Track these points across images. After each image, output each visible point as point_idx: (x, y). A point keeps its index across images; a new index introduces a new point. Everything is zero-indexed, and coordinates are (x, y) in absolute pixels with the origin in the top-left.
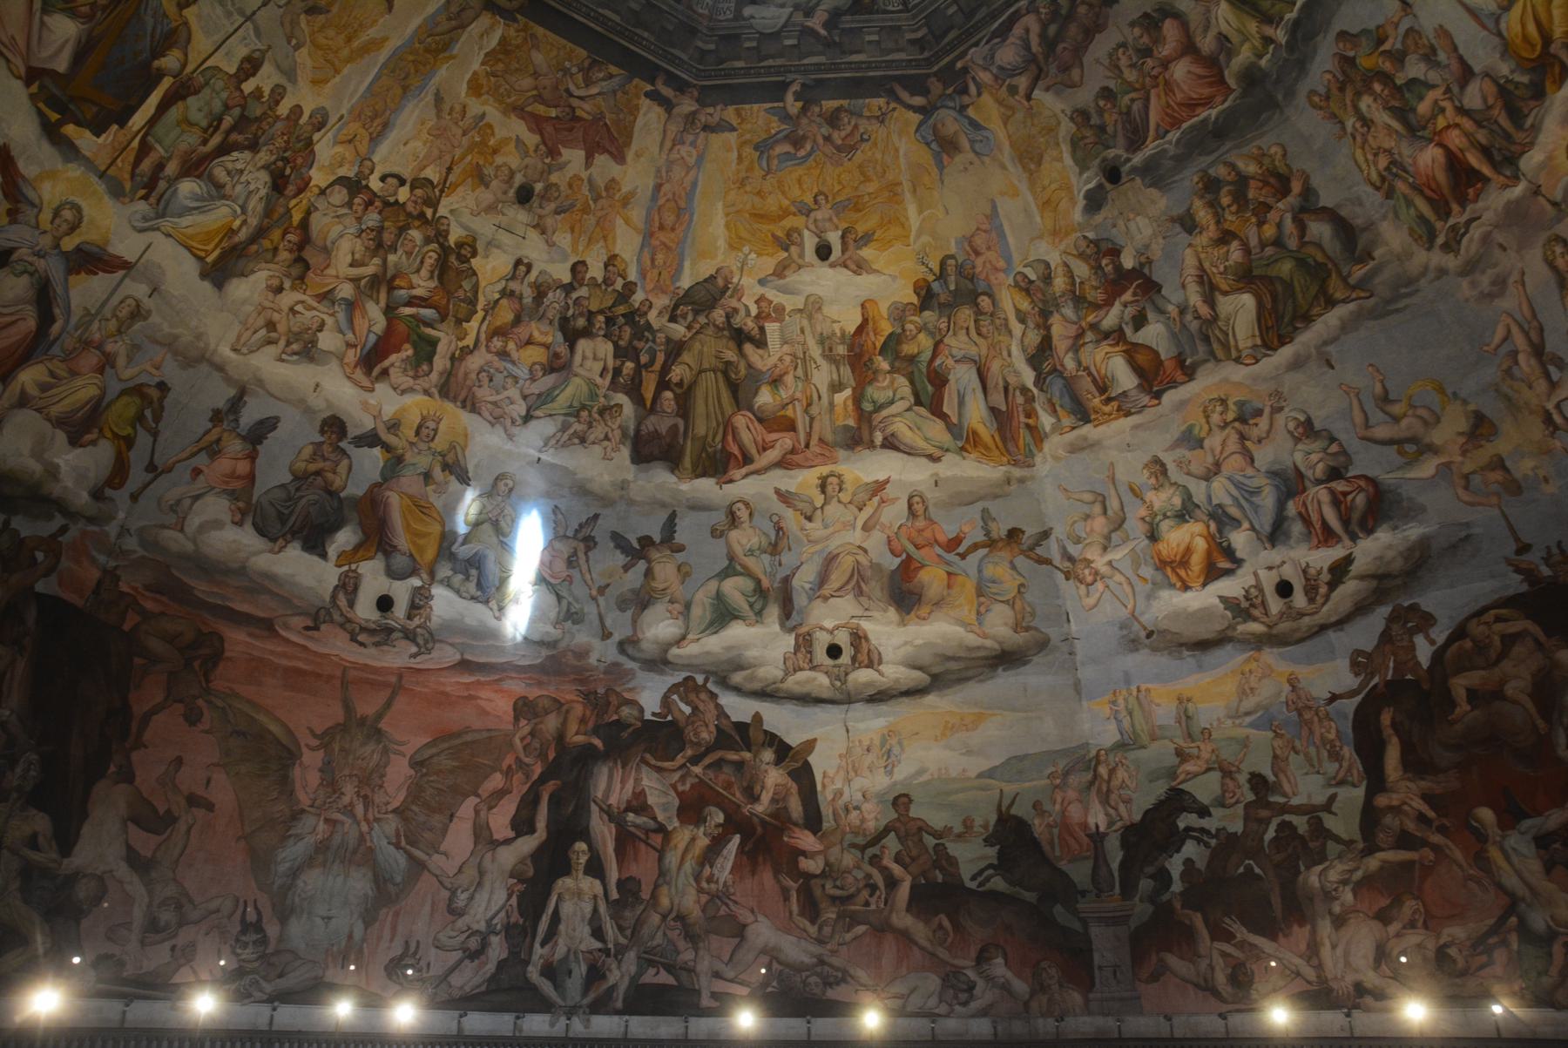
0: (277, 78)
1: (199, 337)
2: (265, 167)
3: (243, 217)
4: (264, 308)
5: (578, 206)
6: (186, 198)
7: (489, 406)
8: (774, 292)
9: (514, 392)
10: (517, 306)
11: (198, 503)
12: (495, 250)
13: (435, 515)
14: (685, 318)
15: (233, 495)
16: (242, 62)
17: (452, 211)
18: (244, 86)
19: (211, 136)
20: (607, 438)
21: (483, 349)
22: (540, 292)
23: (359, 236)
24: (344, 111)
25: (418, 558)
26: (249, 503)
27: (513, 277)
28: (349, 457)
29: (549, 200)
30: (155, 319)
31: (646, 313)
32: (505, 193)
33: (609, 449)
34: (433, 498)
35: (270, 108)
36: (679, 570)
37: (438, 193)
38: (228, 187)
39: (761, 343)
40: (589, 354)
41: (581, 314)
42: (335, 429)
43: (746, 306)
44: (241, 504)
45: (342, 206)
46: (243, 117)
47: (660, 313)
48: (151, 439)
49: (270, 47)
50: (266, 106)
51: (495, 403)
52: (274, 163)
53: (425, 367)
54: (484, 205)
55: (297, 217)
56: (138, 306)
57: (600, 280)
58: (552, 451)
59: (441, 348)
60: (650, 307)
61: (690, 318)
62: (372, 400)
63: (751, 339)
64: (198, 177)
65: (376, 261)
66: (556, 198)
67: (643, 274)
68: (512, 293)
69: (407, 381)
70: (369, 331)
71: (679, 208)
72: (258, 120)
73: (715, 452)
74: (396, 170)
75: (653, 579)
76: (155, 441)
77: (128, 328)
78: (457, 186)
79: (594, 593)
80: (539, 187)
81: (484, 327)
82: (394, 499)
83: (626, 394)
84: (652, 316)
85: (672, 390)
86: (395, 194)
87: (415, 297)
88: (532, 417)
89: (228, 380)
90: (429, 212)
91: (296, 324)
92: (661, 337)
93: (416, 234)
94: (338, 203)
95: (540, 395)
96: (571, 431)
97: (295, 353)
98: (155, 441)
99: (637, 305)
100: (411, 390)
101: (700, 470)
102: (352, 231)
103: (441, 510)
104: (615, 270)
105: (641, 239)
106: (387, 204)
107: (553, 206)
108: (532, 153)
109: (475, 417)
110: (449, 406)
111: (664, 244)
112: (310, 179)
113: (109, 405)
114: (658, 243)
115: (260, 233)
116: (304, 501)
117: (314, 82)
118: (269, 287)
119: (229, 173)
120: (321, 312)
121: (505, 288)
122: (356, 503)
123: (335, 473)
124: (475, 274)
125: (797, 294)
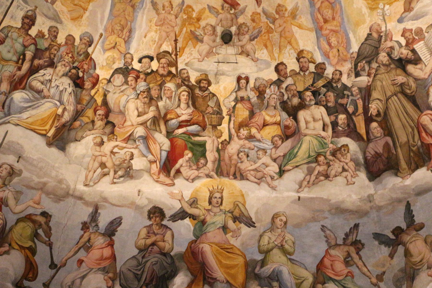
0: (49, 23)
1: (60, 181)
2: (64, 75)
3: (63, 107)
4: (96, 156)
5: (264, 31)
6: (21, 102)
7: (252, 172)
8: (411, 22)
9: (266, 159)
10: (249, 106)
11: (85, 280)
12: (222, 77)
13: (238, 252)
14: (364, 70)
15: (104, 270)
16: (23, 20)
17: (186, 64)
18: (30, 32)
19: (22, 64)
20: (344, 170)
21: (236, 138)
22: (261, 93)
23: (138, 98)
24: (101, 31)
25: (232, 282)
26: (115, 273)
27: (239, 89)
28: (171, 229)
29: (243, 34)
30: (25, 174)
31: (339, 79)
32: (214, 41)
33: (349, 178)
34: (233, 241)
35: (53, 41)
36: (426, 242)
37: (173, 56)
38: (45, 91)
39: (417, 60)
40: (309, 119)
41: (294, 96)
42: (157, 215)
43: (397, 42)
44: (111, 275)
45: (122, 85)
46: (37, 49)
47: (349, 75)
48: (48, 248)
49: (36, 7)
50: (49, 41)
51: (256, 170)
52: (70, 71)
53: (202, 161)
54: (204, 53)
55: (99, 100)
56: (12, 168)
57: (298, 70)
58: (306, 189)
59: (209, 146)
60: (341, 74)
61: (367, 68)
62: (175, 190)
63: (409, 62)
64: (24, 88)
65: (153, 108)
66: (248, 32)
67: (326, 55)
68: (242, 99)
69: (194, 173)
70: (161, 150)
71: (331, 3)
72: (46, 49)
73: (418, 149)
74: (145, 53)
75: (411, 256)
76: (51, 249)
77: (10, 182)
78: (183, 49)
79: (374, 280)
80: (233, 29)
81: (232, 125)
82: (207, 248)
83: (347, 136)
84: (345, 79)
85: (375, 121)
86: (150, 67)
87: (182, 121)
88: (284, 171)
89: (87, 203)
90: (173, 70)
91: (117, 160)
92: (355, 90)
93: (170, 85)
94: (120, 84)
95: (284, 156)
96: (316, 172)
97: (121, 177)
98: (51, 249)
99: (330, 76)
100: (198, 177)
101: (413, 165)
102: (133, 96)
103: (240, 248)
104: (305, 60)
105: (314, 33)
106: (147, 74)
107: (247, 37)
108: (221, 11)
109: (244, 182)
110: (225, 180)
111: (332, 30)
112: (98, 76)
113: (11, 229)
114: (327, 32)
115: (77, 115)
116: (148, 264)
117: (74, 19)
118: (95, 144)
119: (42, 83)
120: (130, 148)
121: (236, 98)
122: (182, 256)
123: (164, 241)
124: (214, 95)
125: (426, 15)
